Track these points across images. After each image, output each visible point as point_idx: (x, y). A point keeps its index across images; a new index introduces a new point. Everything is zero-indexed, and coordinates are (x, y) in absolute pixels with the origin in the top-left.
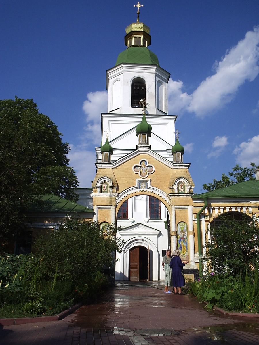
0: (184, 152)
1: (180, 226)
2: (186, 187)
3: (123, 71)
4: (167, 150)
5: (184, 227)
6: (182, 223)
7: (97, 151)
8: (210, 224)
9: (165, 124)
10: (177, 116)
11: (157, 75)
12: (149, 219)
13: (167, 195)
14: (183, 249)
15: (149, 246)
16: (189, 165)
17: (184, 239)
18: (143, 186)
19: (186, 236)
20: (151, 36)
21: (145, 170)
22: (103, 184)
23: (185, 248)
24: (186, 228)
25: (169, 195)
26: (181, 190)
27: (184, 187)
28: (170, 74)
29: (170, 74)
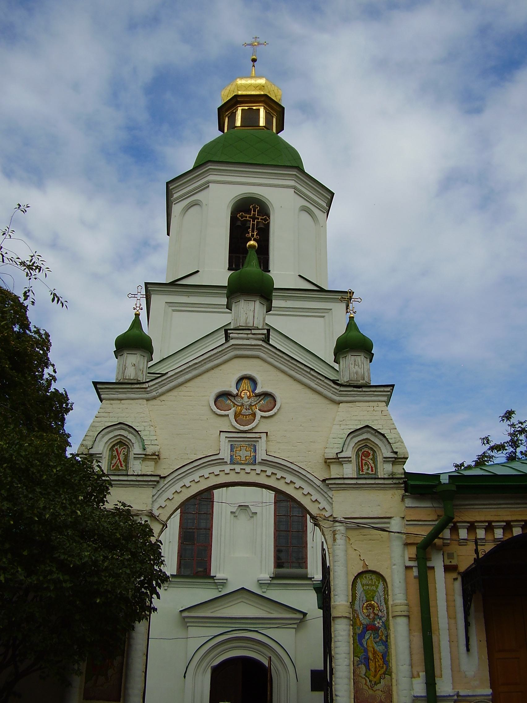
0: (373, 354)
1: (363, 585)
2: (380, 459)
3: (208, 182)
5: (374, 588)
6: (368, 575)
8: (460, 579)
9: (321, 313)
11: (298, 192)
12: (273, 578)
13: (319, 483)
14: (372, 664)
16: (388, 389)
17: (375, 629)
18: (244, 454)
19: (384, 619)
21: (251, 405)
22: (116, 447)
23: (381, 662)
24: (382, 593)
26: (365, 468)
27: (374, 460)
29: (333, 194)
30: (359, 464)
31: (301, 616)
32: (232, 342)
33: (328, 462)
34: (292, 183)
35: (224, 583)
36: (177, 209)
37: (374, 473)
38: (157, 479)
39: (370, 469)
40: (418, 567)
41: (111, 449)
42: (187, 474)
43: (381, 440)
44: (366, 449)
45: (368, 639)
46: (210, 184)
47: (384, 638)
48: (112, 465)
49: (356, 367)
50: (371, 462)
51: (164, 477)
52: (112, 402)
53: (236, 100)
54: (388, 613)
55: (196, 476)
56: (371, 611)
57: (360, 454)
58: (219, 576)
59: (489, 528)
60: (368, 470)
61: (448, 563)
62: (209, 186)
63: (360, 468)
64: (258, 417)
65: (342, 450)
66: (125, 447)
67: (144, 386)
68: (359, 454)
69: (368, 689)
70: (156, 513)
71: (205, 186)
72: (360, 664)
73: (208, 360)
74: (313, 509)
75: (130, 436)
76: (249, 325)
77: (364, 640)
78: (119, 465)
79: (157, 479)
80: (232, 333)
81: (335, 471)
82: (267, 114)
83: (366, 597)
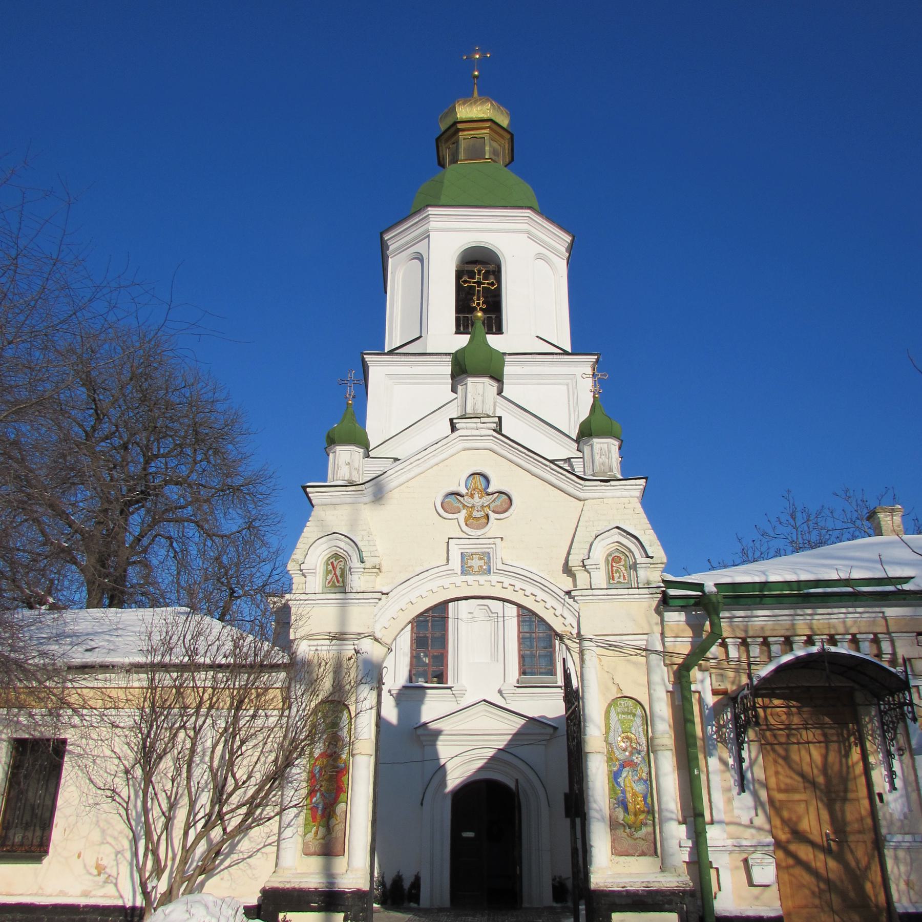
1: (618, 714)
11: (531, 236)
13: (562, 594)
15: (517, 780)
21: (482, 506)
26: (616, 575)
30: (609, 572)
31: (551, 731)
32: (457, 433)
34: (525, 227)
37: (626, 581)
39: (622, 577)
45: (625, 778)
48: (328, 581)
49: (603, 457)
50: (623, 569)
51: (387, 594)
56: (628, 744)
57: (610, 560)
60: (619, 578)
62: (428, 236)
63: (611, 577)
65: (589, 556)
66: (341, 560)
68: (608, 560)
69: (627, 837)
72: (616, 808)
73: (432, 454)
76: (478, 412)
77: (621, 779)
78: (335, 580)
80: (459, 423)
83: (622, 728)
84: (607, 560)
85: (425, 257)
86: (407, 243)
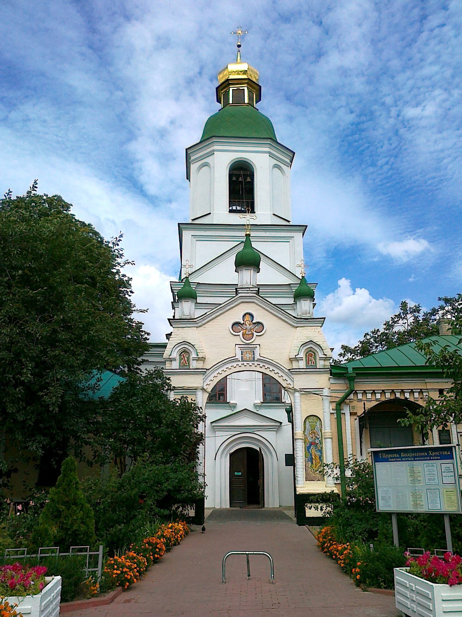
1: (309, 422)
2: (317, 358)
3: (214, 151)
4: (291, 285)
6: (311, 417)
7: (173, 288)
9: (287, 239)
10: (307, 226)
11: (271, 155)
13: (287, 371)
14: (314, 462)
16: (322, 320)
18: (248, 356)
19: (319, 439)
20: (260, 87)
21: (251, 329)
22: (183, 353)
24: (319, 426)
25: (291, 370)
26: (310, 362)
28: (295, 153)
31: (279, 424)
32: (240, 295)
33: (291, 360)
34: (267, 149)
35: (234, 406)
36: (194, 167)
38: (205, 370)
40: (337, 413)
41: (180, 355)
42: (220, 367)
43: (318, 348)
44: (311, 352)
46: (215, 152)
47: (320, 449)
50: (313, 359)
52: (178, 329)
53: (227, 83)
54: (322, 436)
55: (224, 368)
58: (232, 402)
59: (374, 393)
61: (351, 411)
63: (307, 363)
64: (255, 336)
67: (195, 320)
70: (205, 387)
71: (212, 153)
74: (284, 384)
75: (190, 348)
79: (205, 370)
81: (295, 365)
82: (249, 91)
84: (306, 355)
85: (212, 165)
86: (201, 156)
